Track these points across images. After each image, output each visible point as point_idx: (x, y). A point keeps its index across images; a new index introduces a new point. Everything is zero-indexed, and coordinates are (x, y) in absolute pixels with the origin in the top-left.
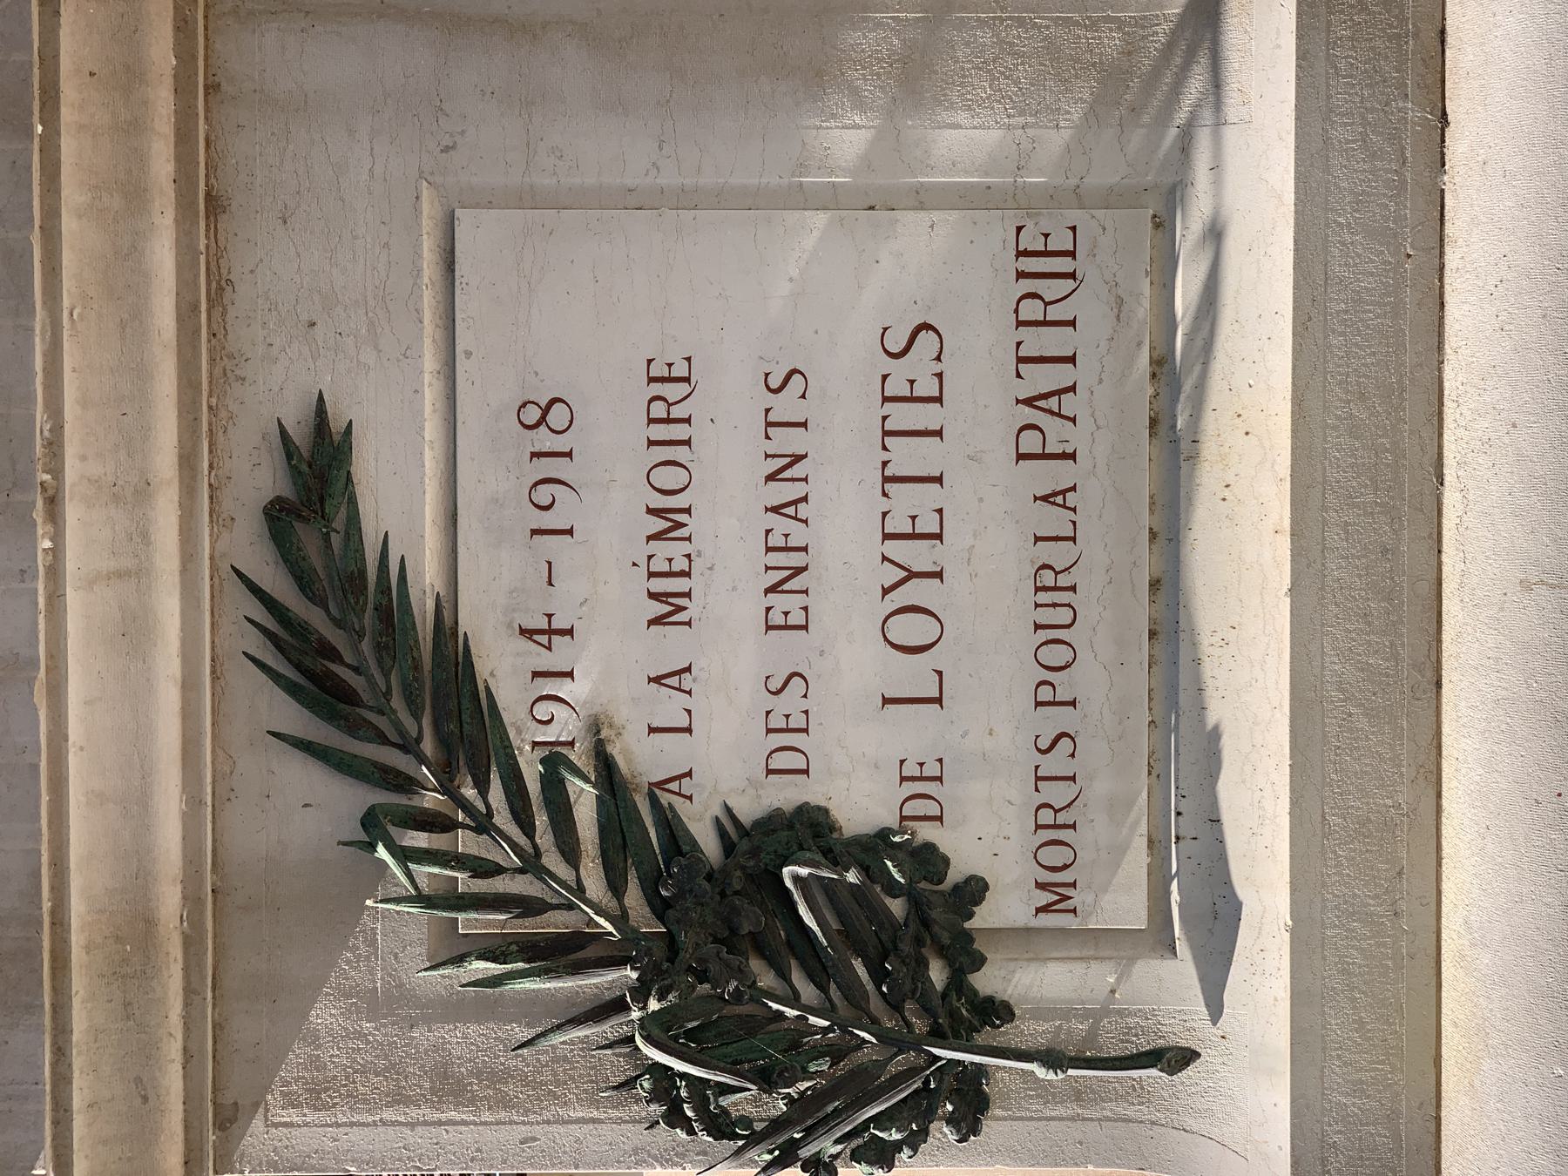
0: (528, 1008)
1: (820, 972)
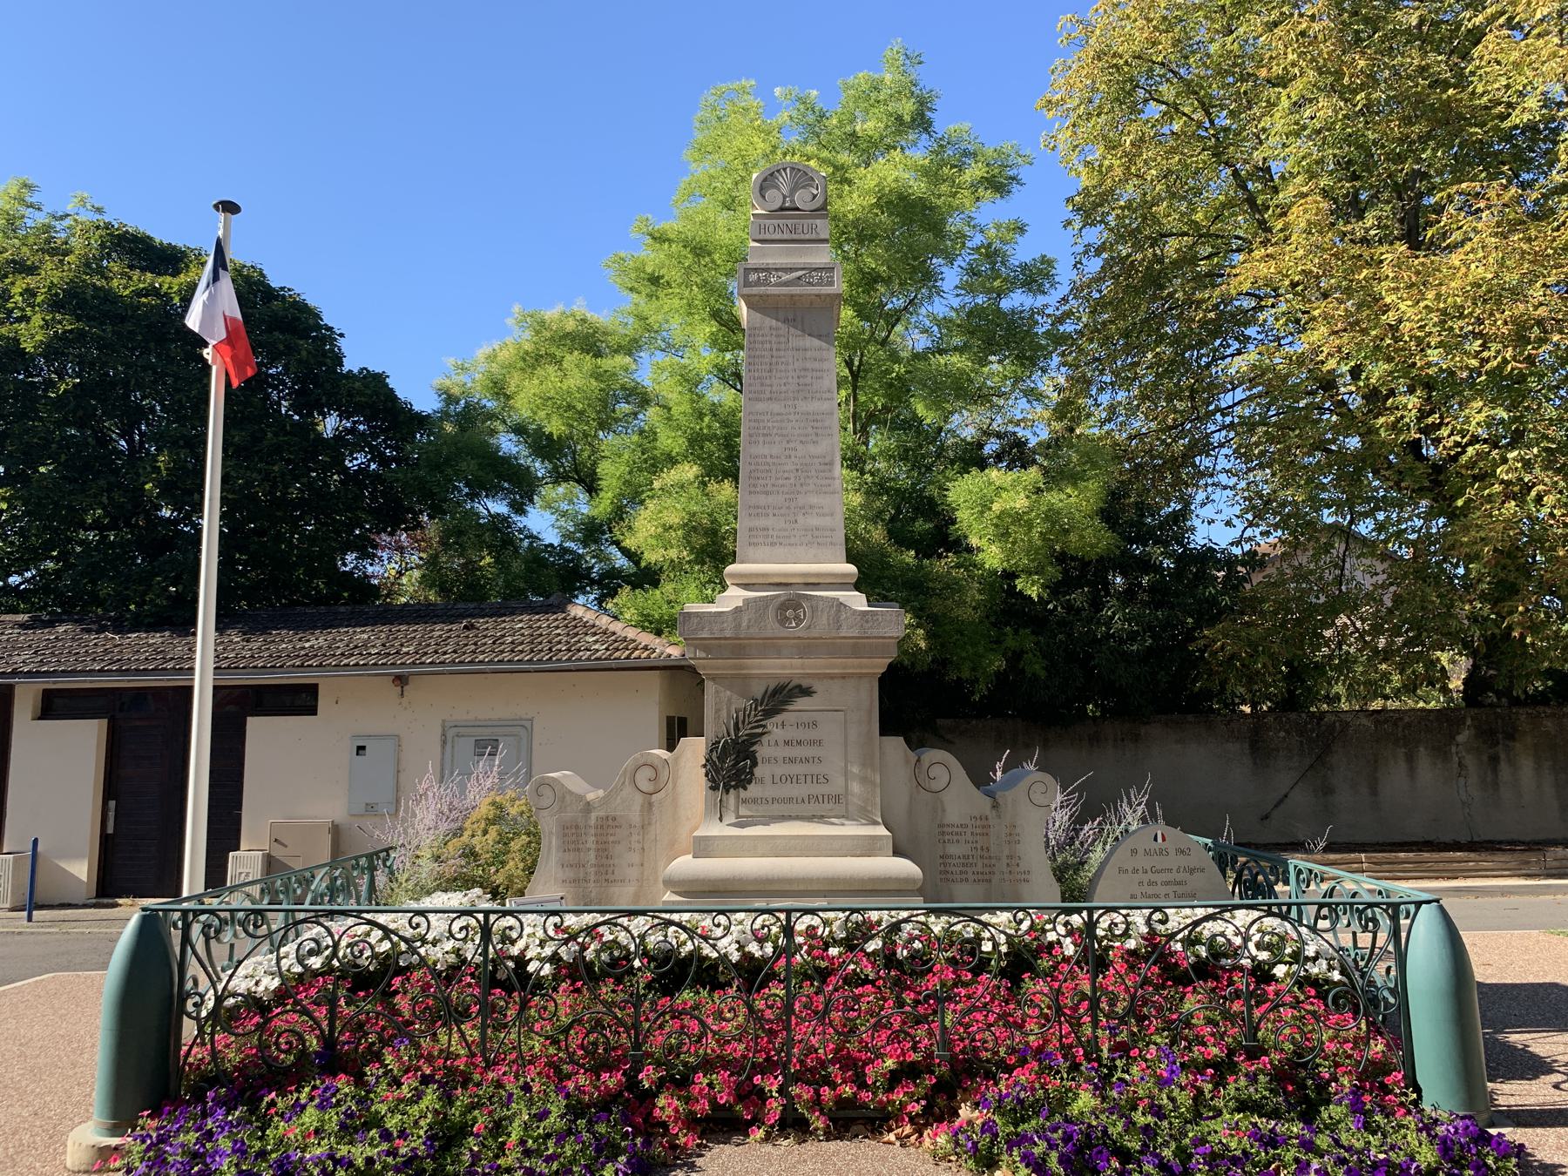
0: (729, 722)
1: (734, 765)
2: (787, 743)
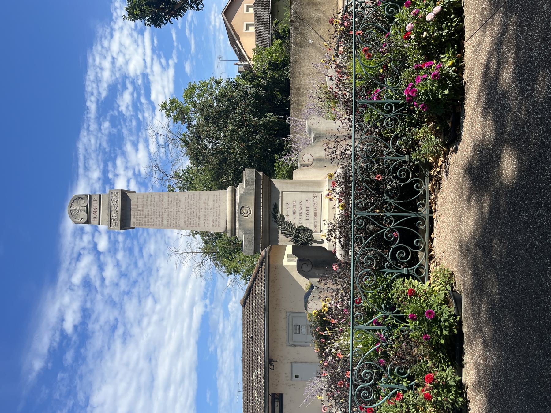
2: (294, 214)
